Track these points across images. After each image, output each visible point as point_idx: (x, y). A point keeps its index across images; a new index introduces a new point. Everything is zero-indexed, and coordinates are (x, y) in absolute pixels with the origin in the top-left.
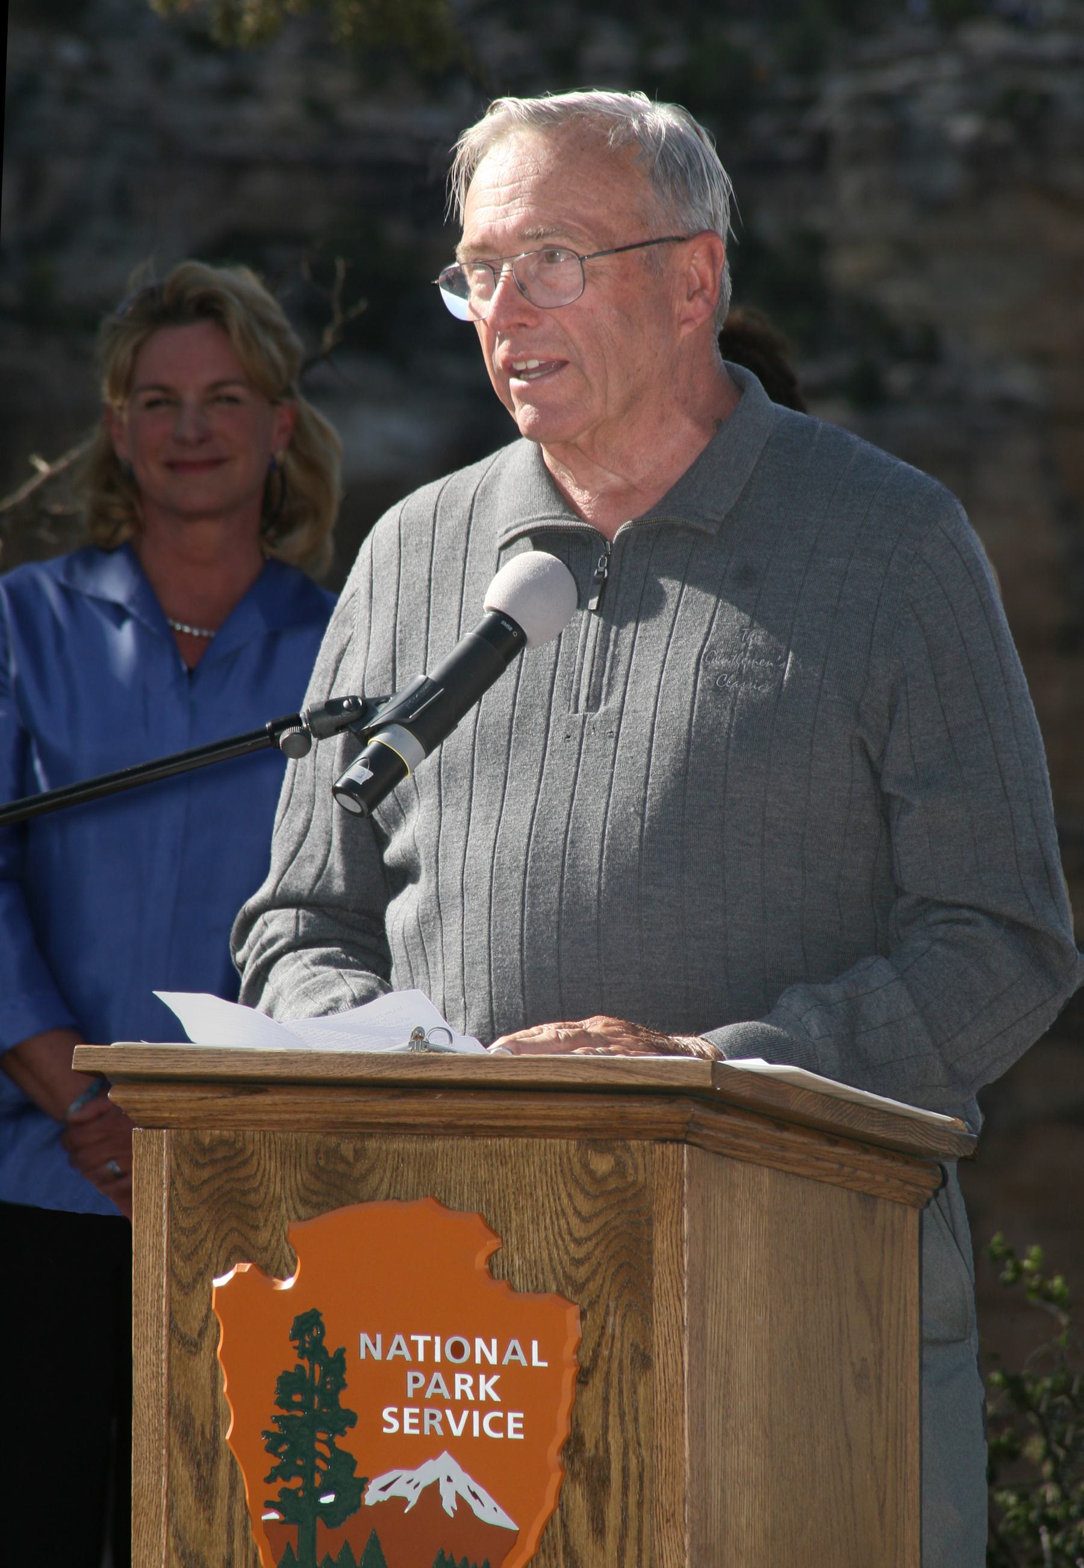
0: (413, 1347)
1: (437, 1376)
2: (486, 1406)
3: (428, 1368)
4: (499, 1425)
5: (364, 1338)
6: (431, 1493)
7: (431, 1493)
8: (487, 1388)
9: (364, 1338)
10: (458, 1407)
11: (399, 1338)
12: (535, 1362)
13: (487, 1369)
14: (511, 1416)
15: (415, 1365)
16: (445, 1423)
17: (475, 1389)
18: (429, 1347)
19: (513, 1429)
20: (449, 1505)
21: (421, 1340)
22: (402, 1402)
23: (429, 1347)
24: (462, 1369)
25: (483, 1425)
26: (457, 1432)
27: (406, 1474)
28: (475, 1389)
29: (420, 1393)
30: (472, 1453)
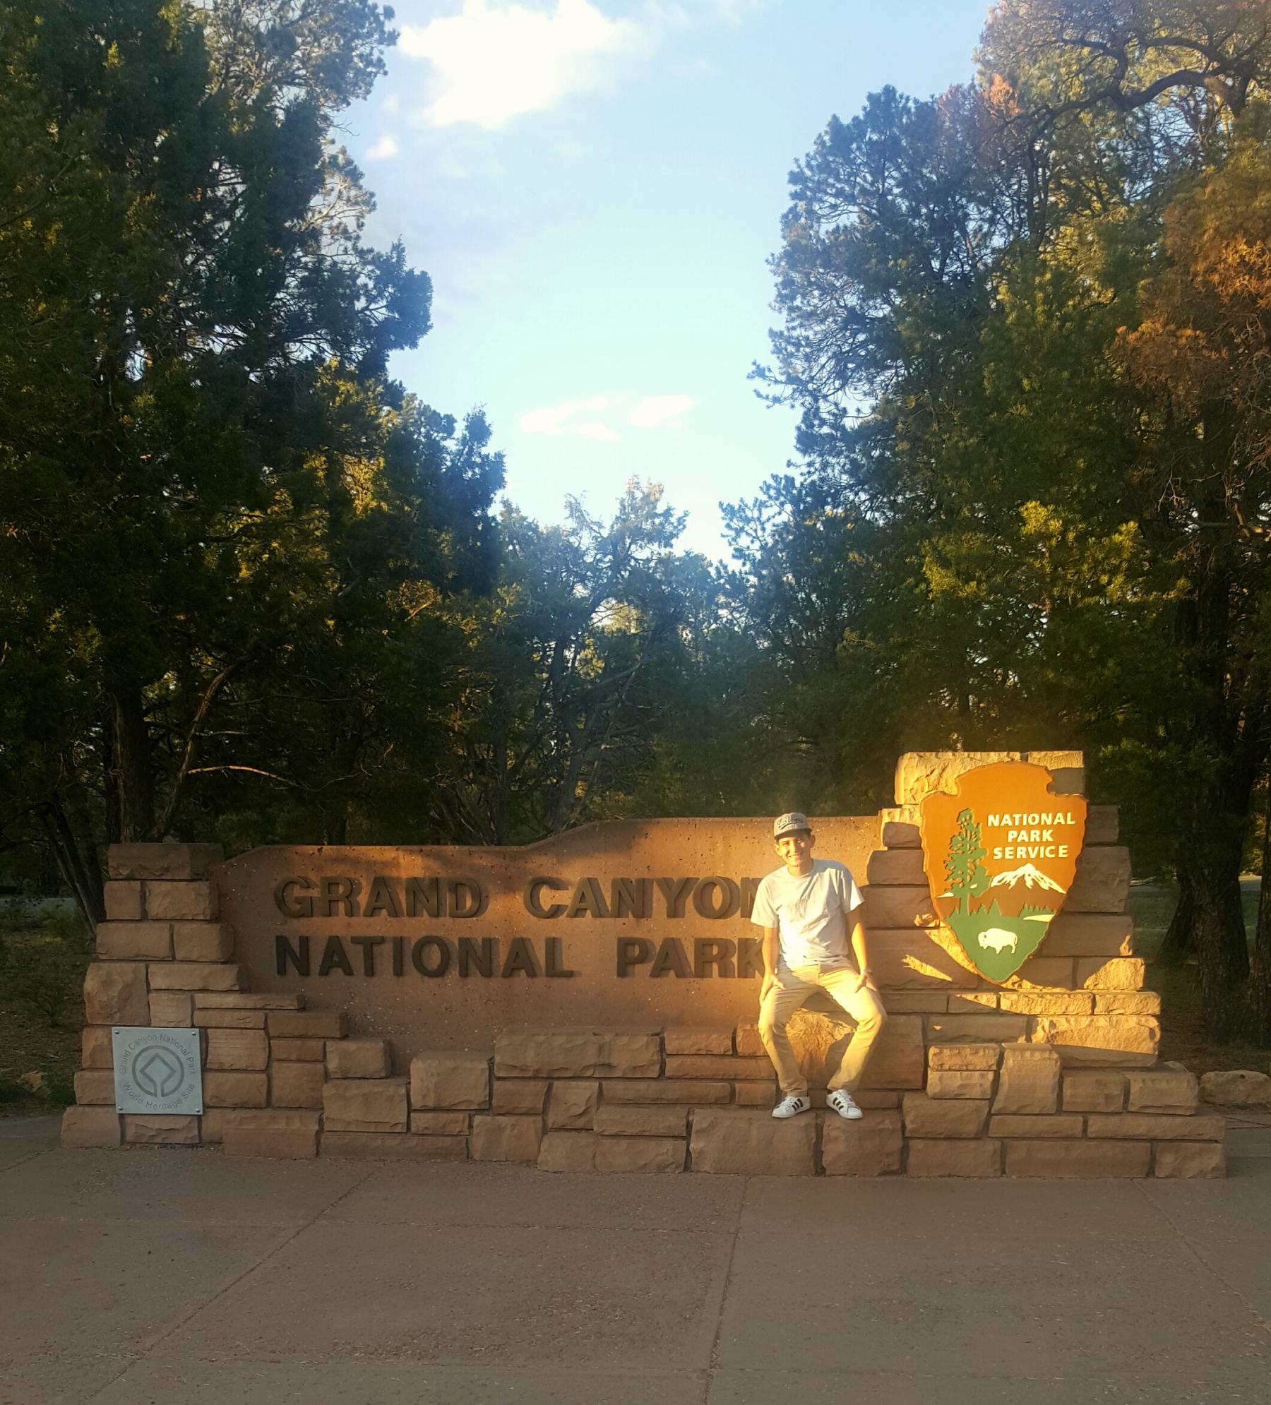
1: (1023, 833)
2: (1047, 844)
3: (1019, 828)
4: (1056, 851)
5: (991, 818)
6: (1022, 880)
7: (1022, 880)
8: (1047, 835)
10: (1034, 844)
11: (1007, 817)
12: (1069, 822)
13: (1047, 827)
15: (1013, 827)
16: (1027, 852)
17: (1041, 836)
18: (1021, 819)
20: (1029, 884)
21: (1017, 816)
22: (1005, 844)
23: (1021, 819)
25: (1046, 852)
26: (1033, 855)
28: (1041, 836)
30: (1039, 863)
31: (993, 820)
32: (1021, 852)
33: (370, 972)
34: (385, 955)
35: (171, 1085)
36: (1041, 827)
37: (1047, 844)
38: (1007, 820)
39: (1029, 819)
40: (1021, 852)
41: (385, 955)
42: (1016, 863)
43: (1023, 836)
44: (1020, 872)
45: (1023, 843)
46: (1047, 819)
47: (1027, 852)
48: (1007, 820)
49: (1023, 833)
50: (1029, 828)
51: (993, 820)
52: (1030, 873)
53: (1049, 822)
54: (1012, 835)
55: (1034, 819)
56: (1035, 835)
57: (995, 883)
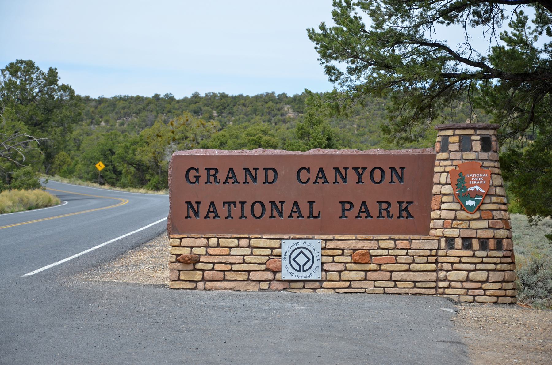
3: (475, 177)
6: (475, 189)
7: (475, 189)
8: (481, 179)
25: (481, 182)
30: (479, 185)
32: (475, 182)
35: (306, 267)
38: (471, 175)
42: (473, 185)
43: (476, 179)
44: (475, 187)
48: (471, 175)
50: (477, 178)
52: (477, 188)
57: (468, 190)
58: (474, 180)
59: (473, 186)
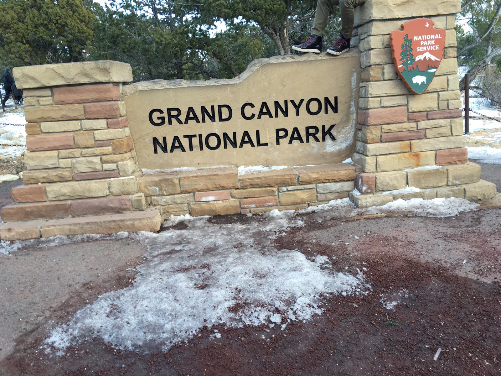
0: (422, 38)
1: (426, 42)
2: (433, 45)
3: (424, 41)
4: (435, 48)
5: (415, 37)
6: (425, 58)
7: (425, 58)
8: (433, 42)
9: (415, 37)
12: (440, 37)
13: (433, 40)
14: (437, 46)
15: (422, 40)
16: (427, 49)
18: (424, 37)
19: (437, 47)
20: (427, 59)
21: (423, 36)
22: (421, 46)
23: (424, 37)
24: (429, 40)
25: (432, 48)
26: (429, 49)
27: (421, 56)
29: (423, 44)
30: (431, 52)
31: (416, 38)
32: (425, 48)
33: (191, 149)
34: (195, 141)
36: (430, 40)
37: (433, 45)
38: (420, 38)
39: (427, 37)
40: (425, 48)
41: (195, 141)
43: (426, 43)
45: (426, 46)
46: (433, 37)
47: (427, 49)
48: (420, 38)
49: (426, 42)
50: (427, 40)
51: (416, 38)
52: (428, 55)
53: (434, 38)
54: (422, 43)
55: (429, 37)
56: (429, 42)
58: (423, 46)
59: (422, 54)
